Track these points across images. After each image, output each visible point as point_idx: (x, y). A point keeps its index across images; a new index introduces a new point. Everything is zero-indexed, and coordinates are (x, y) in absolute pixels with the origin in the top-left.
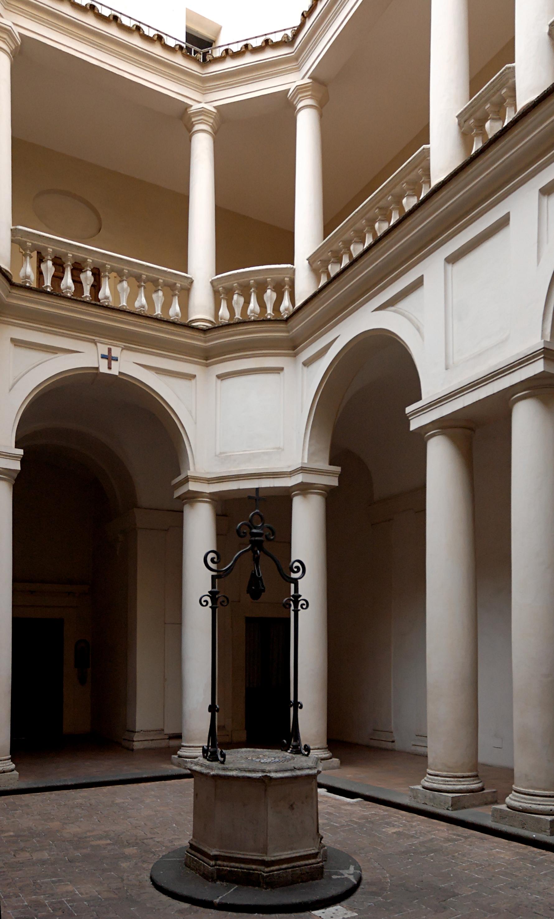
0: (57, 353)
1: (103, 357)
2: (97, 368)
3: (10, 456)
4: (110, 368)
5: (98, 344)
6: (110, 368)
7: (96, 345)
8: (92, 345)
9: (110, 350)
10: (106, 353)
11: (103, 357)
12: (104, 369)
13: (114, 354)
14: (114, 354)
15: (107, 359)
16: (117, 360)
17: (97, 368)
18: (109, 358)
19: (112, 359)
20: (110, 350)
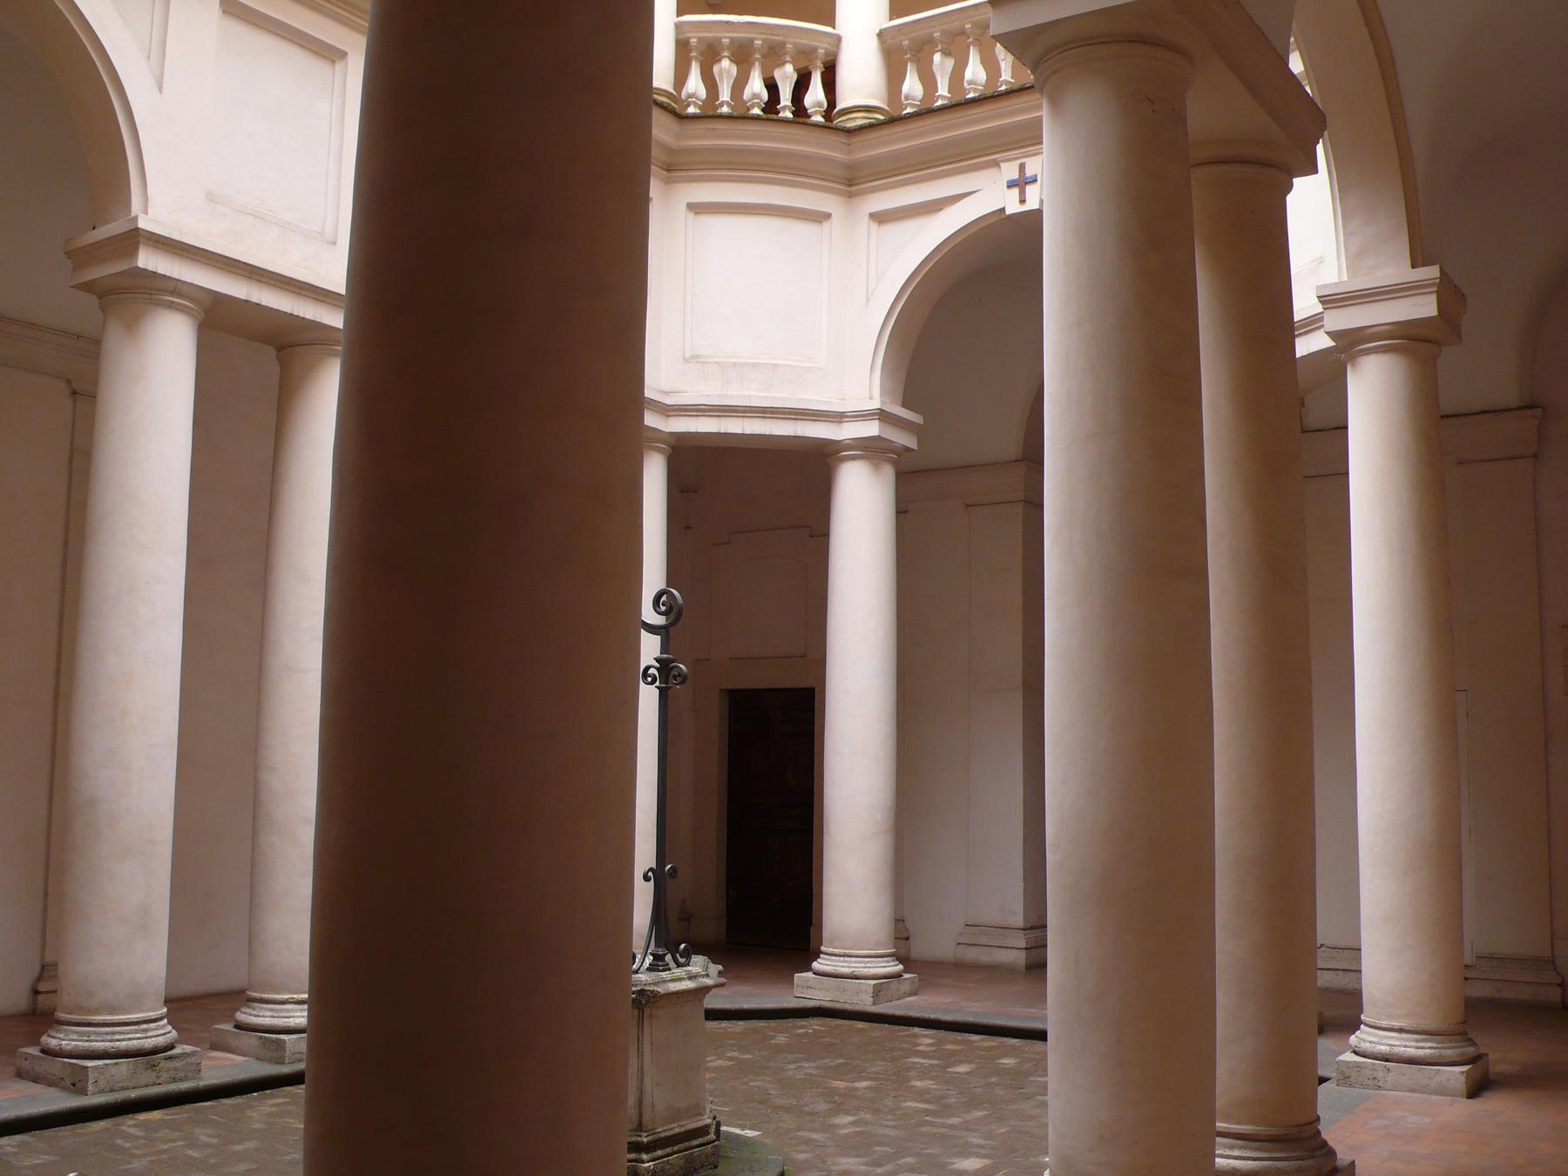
0: (941, 209)
1: (1011, 185)
2: (1003, 210)
3: (862, 416)
4: (1023, 201)
5: (1002, 165)
6: (1023, 201)
7: (1000, 166)
8: (990, 173)
9: (1022, 167)
10: (1015, 175)
11: (1011, 185)
12: (1013, 207)
13: (1029, 173)
14: (1029, 173)
15: (1017, 185)
16: (1036, 181)
17: (1003, 210)
18: (1021, 183)
19: (1026, 183)
20: (1022, 167)
